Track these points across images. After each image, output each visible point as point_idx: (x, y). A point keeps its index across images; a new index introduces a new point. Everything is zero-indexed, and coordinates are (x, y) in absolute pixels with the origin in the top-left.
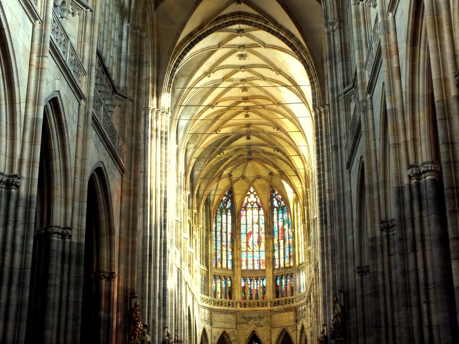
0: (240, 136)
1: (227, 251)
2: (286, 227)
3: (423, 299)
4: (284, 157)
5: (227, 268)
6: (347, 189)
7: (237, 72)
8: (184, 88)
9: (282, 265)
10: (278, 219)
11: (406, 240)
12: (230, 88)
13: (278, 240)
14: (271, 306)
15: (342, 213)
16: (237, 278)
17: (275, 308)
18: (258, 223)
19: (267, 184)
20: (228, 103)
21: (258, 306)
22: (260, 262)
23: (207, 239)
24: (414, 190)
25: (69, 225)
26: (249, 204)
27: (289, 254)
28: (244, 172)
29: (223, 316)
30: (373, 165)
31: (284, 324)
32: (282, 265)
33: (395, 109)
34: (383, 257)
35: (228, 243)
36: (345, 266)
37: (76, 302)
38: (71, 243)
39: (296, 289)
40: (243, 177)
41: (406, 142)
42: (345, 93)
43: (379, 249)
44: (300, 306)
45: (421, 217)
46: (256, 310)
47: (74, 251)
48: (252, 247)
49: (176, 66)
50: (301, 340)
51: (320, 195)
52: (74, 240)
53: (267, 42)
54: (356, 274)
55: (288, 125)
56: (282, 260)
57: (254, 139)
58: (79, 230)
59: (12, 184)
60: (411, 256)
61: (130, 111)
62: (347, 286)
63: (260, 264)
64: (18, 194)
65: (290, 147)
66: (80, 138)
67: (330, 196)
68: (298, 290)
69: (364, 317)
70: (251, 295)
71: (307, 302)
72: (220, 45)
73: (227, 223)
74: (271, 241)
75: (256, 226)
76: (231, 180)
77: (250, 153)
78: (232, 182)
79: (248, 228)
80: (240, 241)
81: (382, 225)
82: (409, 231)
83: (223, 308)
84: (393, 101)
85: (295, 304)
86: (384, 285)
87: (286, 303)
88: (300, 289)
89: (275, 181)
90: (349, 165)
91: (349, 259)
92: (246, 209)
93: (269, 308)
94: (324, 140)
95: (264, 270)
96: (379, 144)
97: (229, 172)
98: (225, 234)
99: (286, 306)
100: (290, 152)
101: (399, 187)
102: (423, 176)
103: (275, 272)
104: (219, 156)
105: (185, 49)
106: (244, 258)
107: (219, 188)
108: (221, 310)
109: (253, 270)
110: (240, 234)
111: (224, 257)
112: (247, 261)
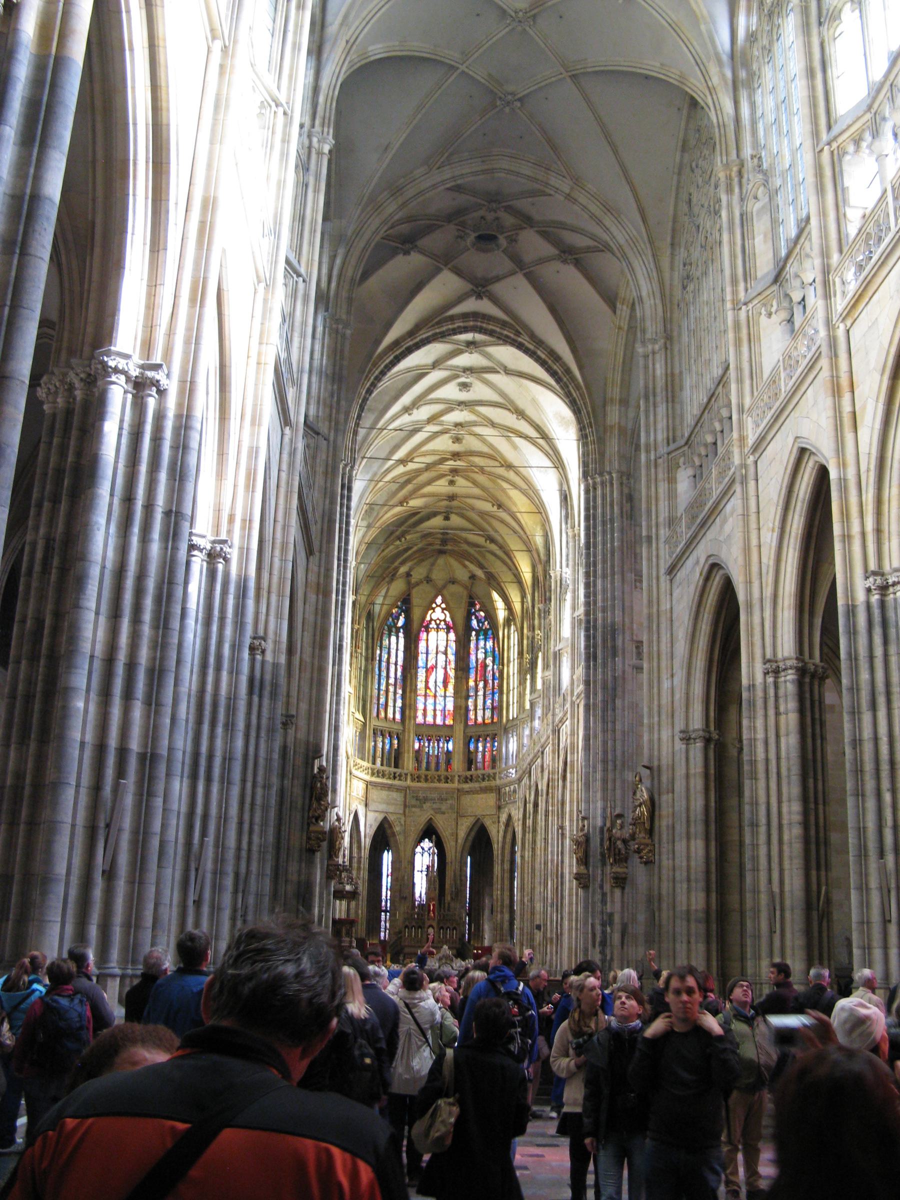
0: (435, 514)
1: (395, 693)
2: (489, 661)
3: (885, 784)
4: (499, 553)
5: (394, 718)
6: (665, 606)
7: (452, 410)
8: (372, 428)
9: (480, 720)
10: (477, 649)
11: (858, 690)
12: (436, 435)
13: (476, 681)
15: (655, 643)
17: (466, 786)
18: (445, 653)
19: (465, 593)
20: (429, 459)
21: (439, 781)
23: (366, 672)
24: (876, 612)
25: (261, 633)
28: (430, 571)
29: (384, 794)
30: (755, 568)
31: (479, 812)
32: (480, 720)
33: (845, 480)
34: (766, 716)
36: (656, 728)
37: (269, 760)
38: (263, 662)
39: (501, 759)
40: (428, 580)
41: (863, 534)
42: (668, 454)
43: (759, 703)
44: (506, 785)
45: (886, 655)
46: (436, 788)
47: (268, 677)
49: (369, 392)
50: (504, 837)
51: (587, 613)
52: (269, 657)
53: (511, 365)
54: (677, 739)
55: (519, 502)
57: (455, 520)
58: (276, 642)
59: (219, 556)
60: (867, 717)
61: (324, 457)
62: (659, 760)
64: (227, 574)
65: (515, 536)
66: (282, 490)
67: (604, 619)
69: (688, 809)
70: (428, 763)
71: (520, 780)
72: (435, 365)
75: (442, 658)
76: (409, 583)
77: (444, 542)
78: (410, 586)
80: (416, 678)
81: (768, 666)
82: (865, 676)
83: (384, 781)
84: (842, 465)
85: (498, 782)
86: (767, 760)
87: (483, 779)
88: (507, 758)
89: (479, 589)
90: (672, 570)
91: (664, 717)
92: (427, 629)
93: (456, 785)
94: (599, 528)
95: (451, 726)
96: (769, 538)
99: (484, 784)
100: (514, 544)
101: (848, 605)
102: (891, 590)
103: (468, 730)
104: (398, 542)
105: (386, 367)
106: (420, 706)
107: (390, 593)
109: (435, 725)
110: (417, 668)
111: (391, 703)
112: (425, 710)
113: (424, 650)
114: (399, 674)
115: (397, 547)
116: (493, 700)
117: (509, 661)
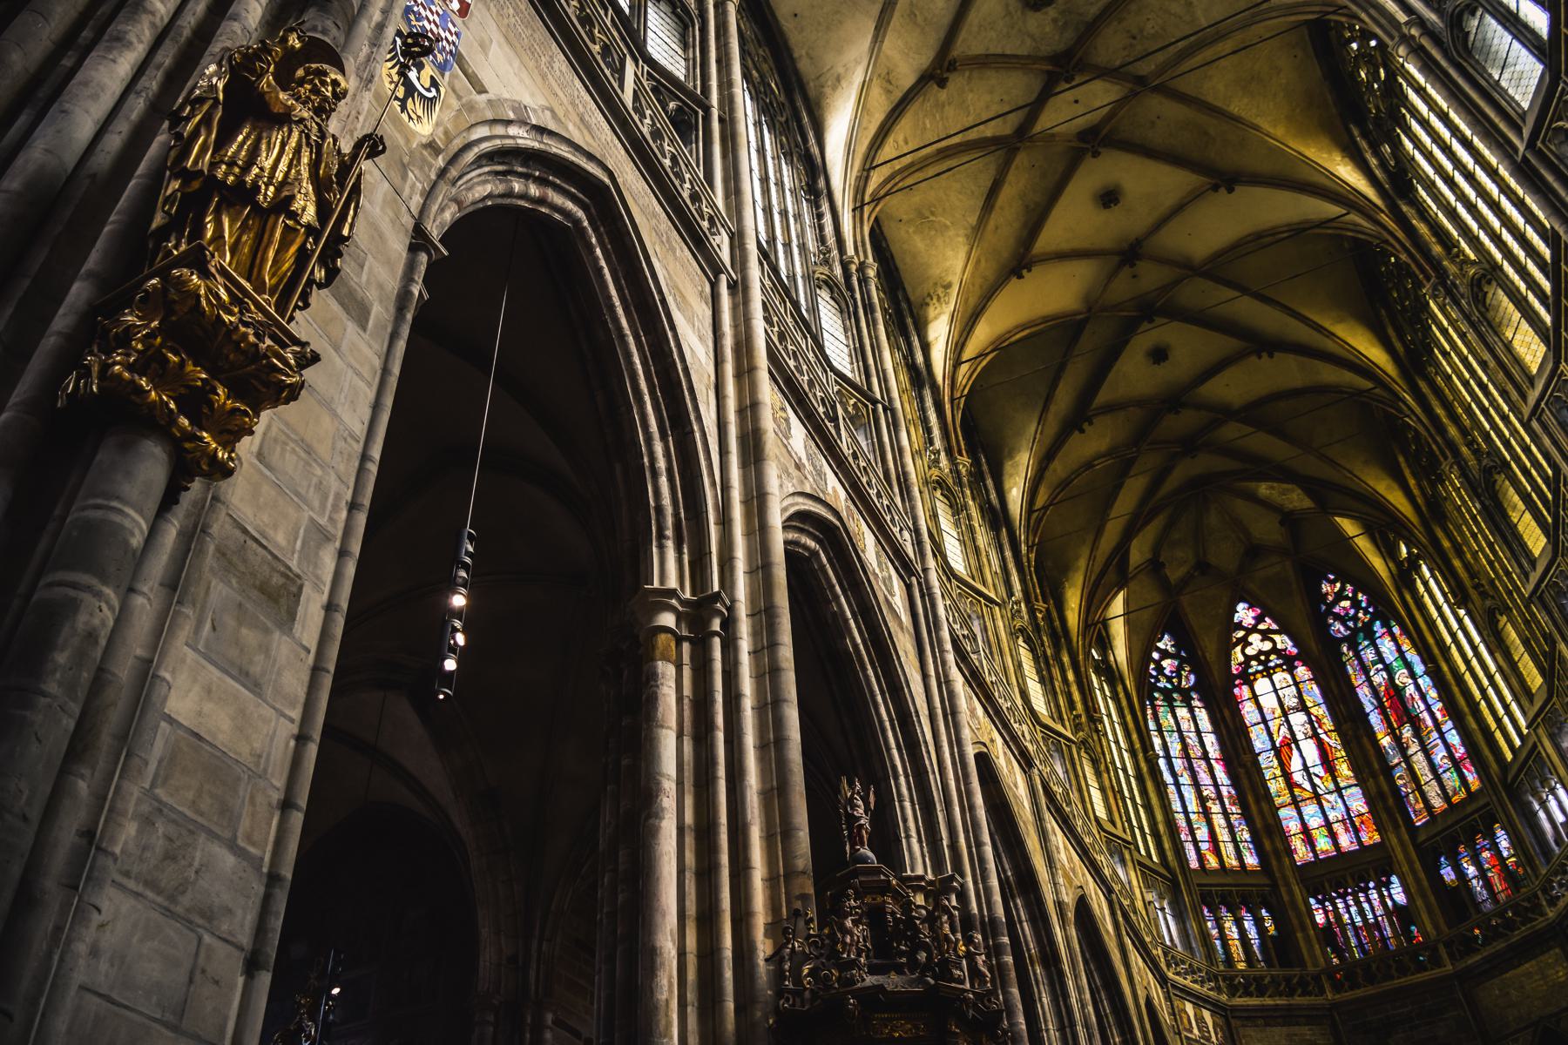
2: (1402, 677)
9: (1438, 803)
10: (1365, 670)
14: (1452, 956)
16: (1291, 892)
18: (1302, 707)
21: (1403, 971)
22: (1353, 823)
26: (1254, 663)
27: (1451, 756)
32: (1438, 803)
35: (1224, 791)
48: (1307, 785)
56: (1432, 791)
63: (1357, 831)
68: (1539, 861)
70: (1360, 945)
73: (1198, 732)
74: (1365, 740)
75: (1298, 719)
76: (1164, 585)
77: (1189, 445)
79: (1274, 729)
87: (1510, 925)
97: (1148, 556)
98: (1202, 763)
99: (1516, 936)
103: (1422, 838)
106: (1293, 826)
108: (1263, 1008)
110: (1255, 756)
111: (1223, 835)
113: (1256, 717)
114: (1222, 776)
115: (1089, 465)
116: (1447, 746)
117: (1445, 650)
